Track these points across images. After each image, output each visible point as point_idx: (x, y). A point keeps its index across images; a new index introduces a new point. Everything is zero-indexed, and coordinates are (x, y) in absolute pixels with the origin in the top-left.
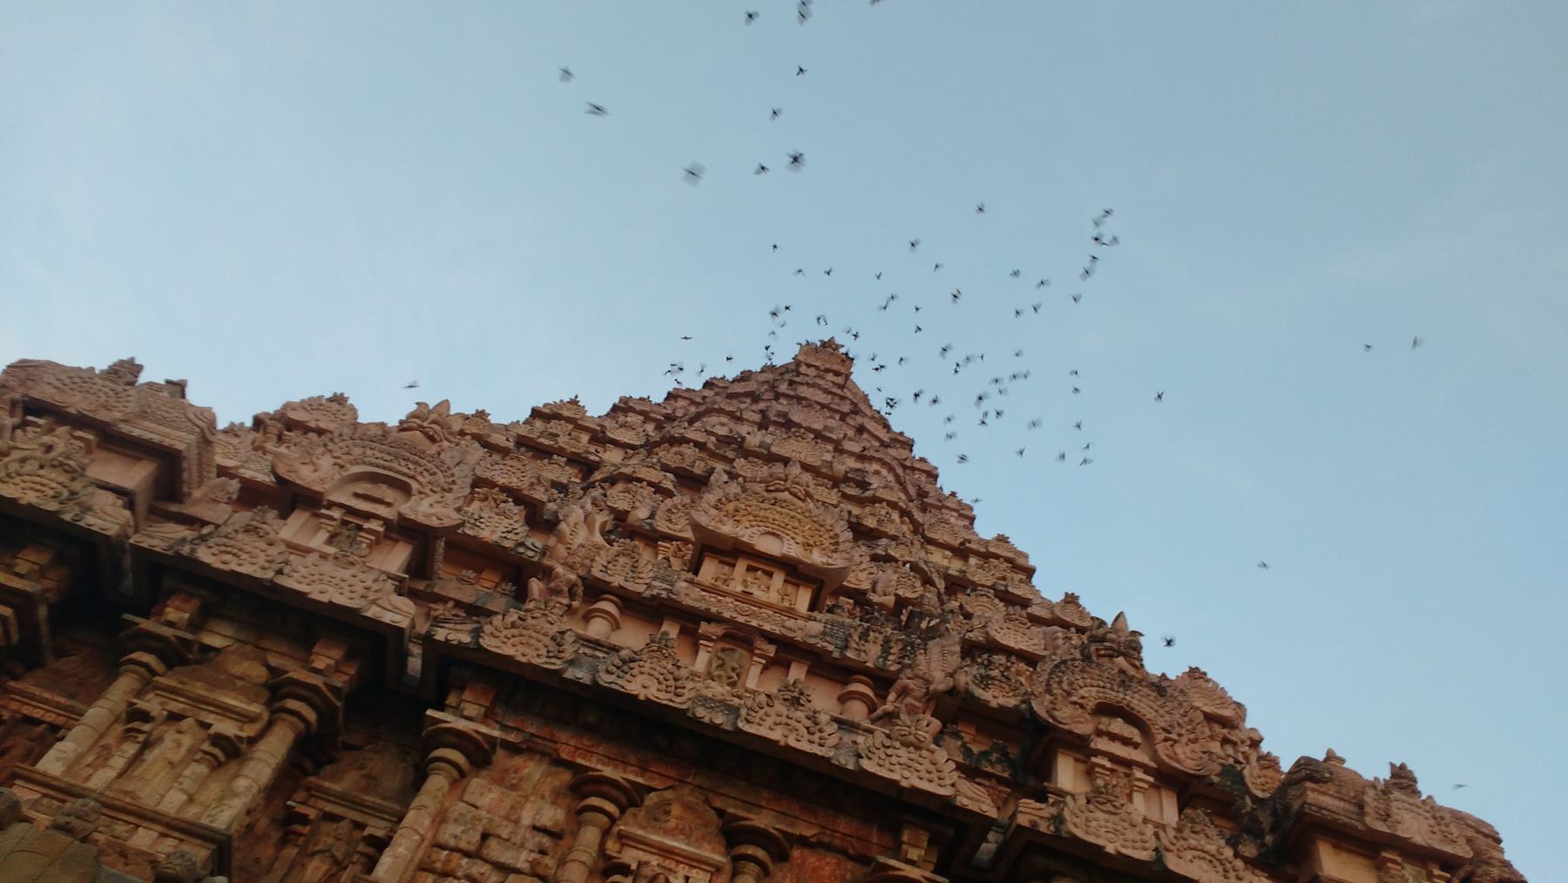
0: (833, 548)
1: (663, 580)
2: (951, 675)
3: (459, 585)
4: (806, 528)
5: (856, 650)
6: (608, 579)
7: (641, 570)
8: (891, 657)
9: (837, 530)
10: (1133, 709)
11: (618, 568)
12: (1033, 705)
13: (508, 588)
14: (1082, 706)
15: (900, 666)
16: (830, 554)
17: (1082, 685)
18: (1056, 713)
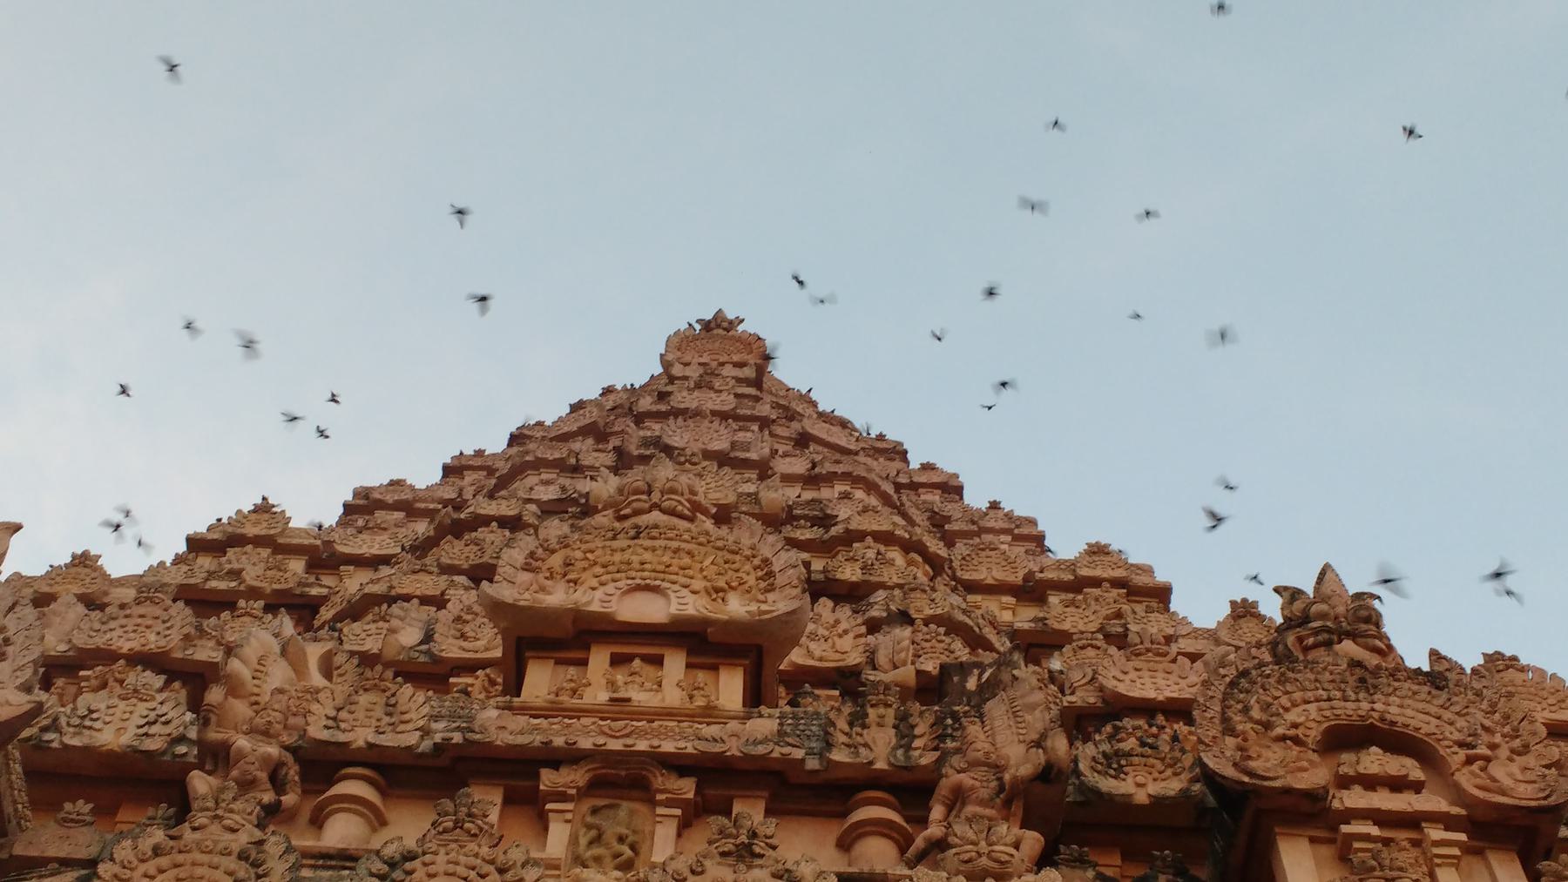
0: (763, 585)
1: (452, 717)
2: (1038, 744)
3: (62, 832)
4: (707, 562)
5: (848, 746)
6: (342, 737)
7: (403, 709)
8: (917, 743)
9: (766, 552)
10: (1393, 723)
11: (360, 715)
12: (1205, 760)
13: (160, 812)
14: (1297, 741)
15: (937, 754)
16: (761, 597)
17: (1288, 705)
18: (1252, 764)
